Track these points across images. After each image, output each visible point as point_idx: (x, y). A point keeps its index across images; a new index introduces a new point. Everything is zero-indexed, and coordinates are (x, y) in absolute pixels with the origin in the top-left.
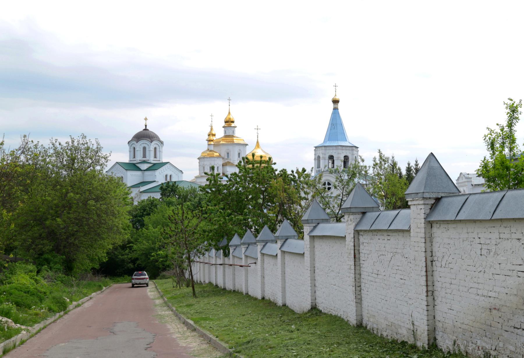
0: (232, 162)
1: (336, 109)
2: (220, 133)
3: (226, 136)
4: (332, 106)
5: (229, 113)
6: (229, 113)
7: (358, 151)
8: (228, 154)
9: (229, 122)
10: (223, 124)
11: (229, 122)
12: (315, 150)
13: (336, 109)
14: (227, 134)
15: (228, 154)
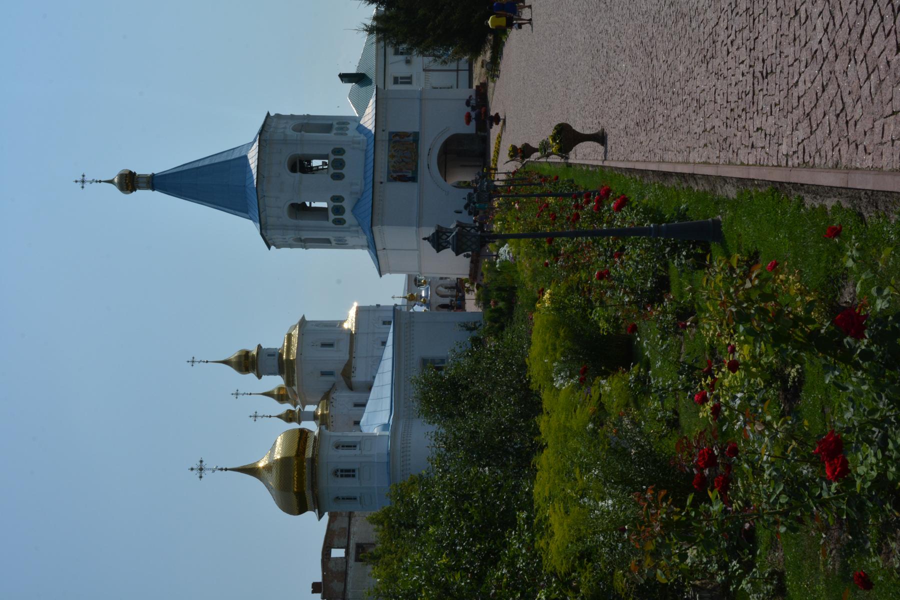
0: (341, 367)
1: (155, 182)
2: (276, 382)
3: (280, 372)
4: (142, 195)
5: (226, 362)
6: (226, 362)
7: (278, 116)
8: (324, 374)
9: (246, 363)
10: (252, 376)
11: (246, 363)
12: (278, 247)
13: (155, 182)
14: (276, 369)
15: (324, 374)
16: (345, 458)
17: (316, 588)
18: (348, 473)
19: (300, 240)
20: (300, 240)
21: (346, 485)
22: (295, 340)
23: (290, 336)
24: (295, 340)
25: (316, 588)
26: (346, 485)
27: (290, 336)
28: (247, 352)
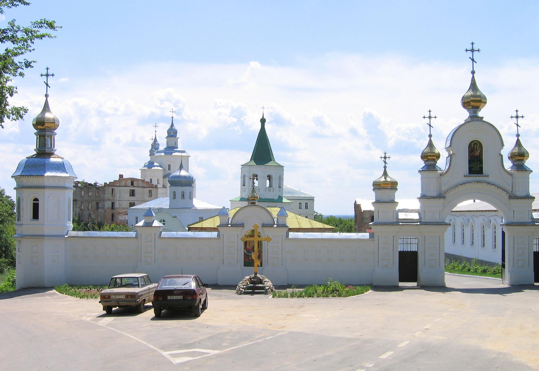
2: (163, 144)
9: (172, 133)
11: (172, 133)
14: (170, 145)
16: (187, 195)
17: (121, 176)
18: (183, 196)
19: (244, 176)
20: (244, 176)
21: (179, 195)
22: (183, 154)
23: (184, 152)
24: (183, 154)
25: (121, 176)
26: (179, 195)
27: (184, 152)
28: (176, 133)
